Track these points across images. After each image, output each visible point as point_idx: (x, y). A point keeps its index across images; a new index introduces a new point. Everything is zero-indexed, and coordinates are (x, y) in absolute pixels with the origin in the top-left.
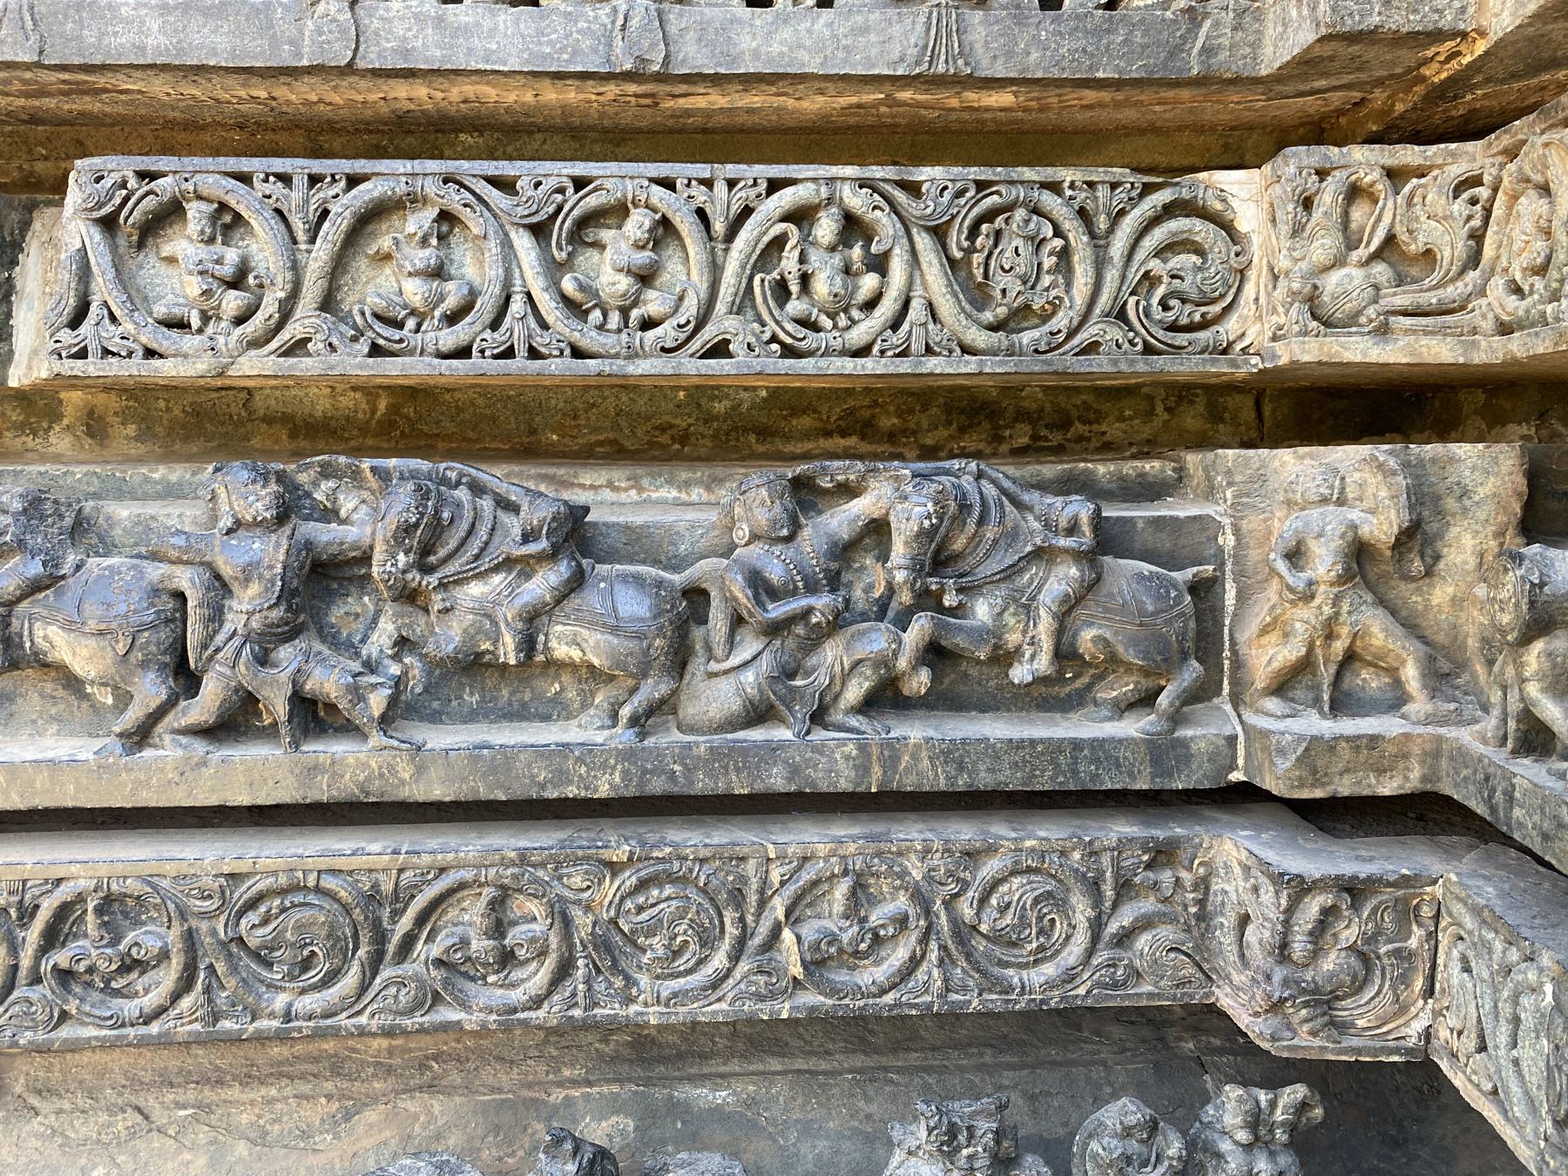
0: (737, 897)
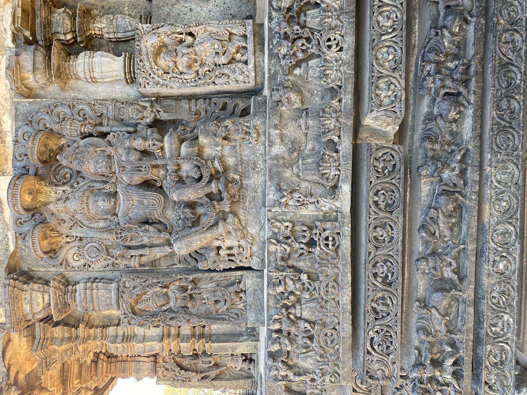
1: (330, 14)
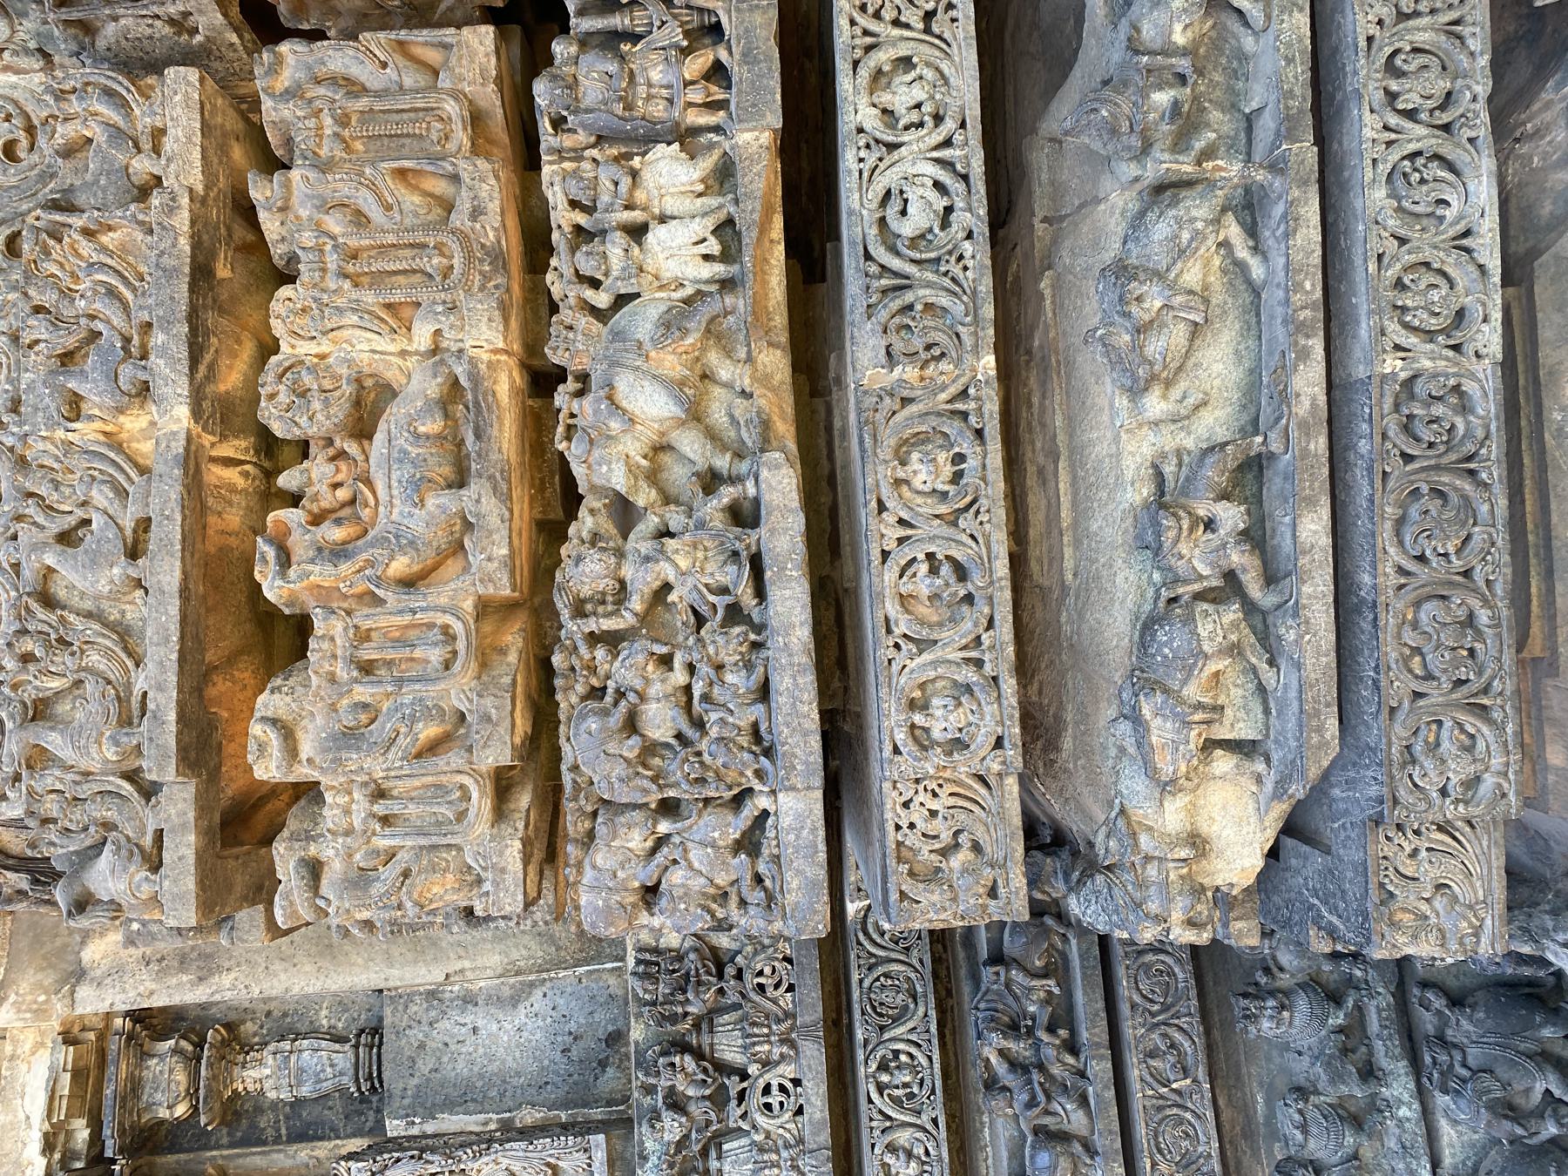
0: (1160, 1109)
1: (774, 1157)
